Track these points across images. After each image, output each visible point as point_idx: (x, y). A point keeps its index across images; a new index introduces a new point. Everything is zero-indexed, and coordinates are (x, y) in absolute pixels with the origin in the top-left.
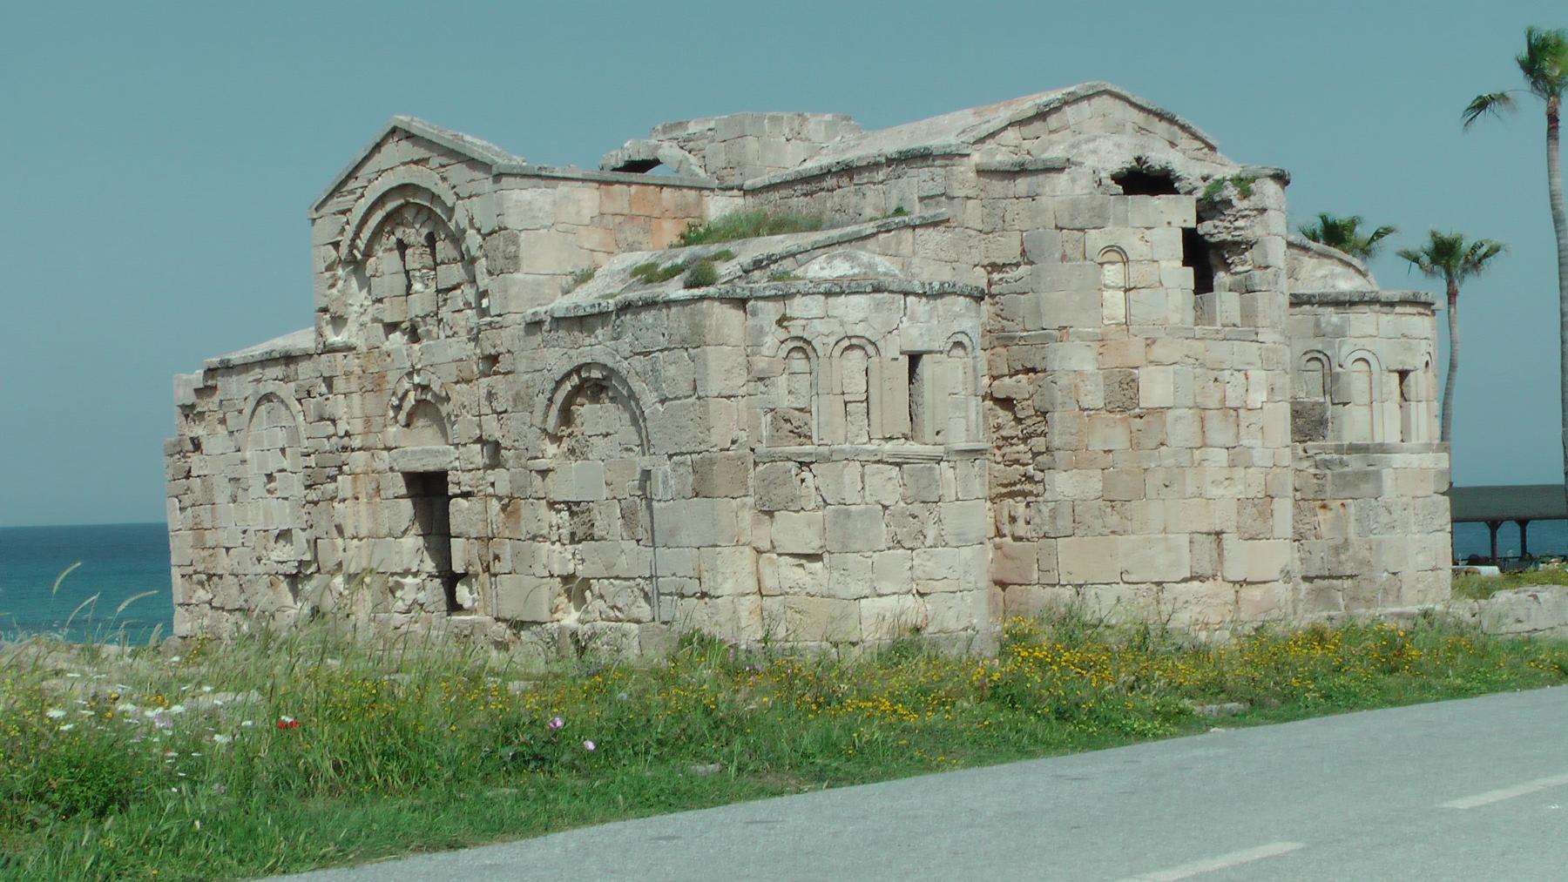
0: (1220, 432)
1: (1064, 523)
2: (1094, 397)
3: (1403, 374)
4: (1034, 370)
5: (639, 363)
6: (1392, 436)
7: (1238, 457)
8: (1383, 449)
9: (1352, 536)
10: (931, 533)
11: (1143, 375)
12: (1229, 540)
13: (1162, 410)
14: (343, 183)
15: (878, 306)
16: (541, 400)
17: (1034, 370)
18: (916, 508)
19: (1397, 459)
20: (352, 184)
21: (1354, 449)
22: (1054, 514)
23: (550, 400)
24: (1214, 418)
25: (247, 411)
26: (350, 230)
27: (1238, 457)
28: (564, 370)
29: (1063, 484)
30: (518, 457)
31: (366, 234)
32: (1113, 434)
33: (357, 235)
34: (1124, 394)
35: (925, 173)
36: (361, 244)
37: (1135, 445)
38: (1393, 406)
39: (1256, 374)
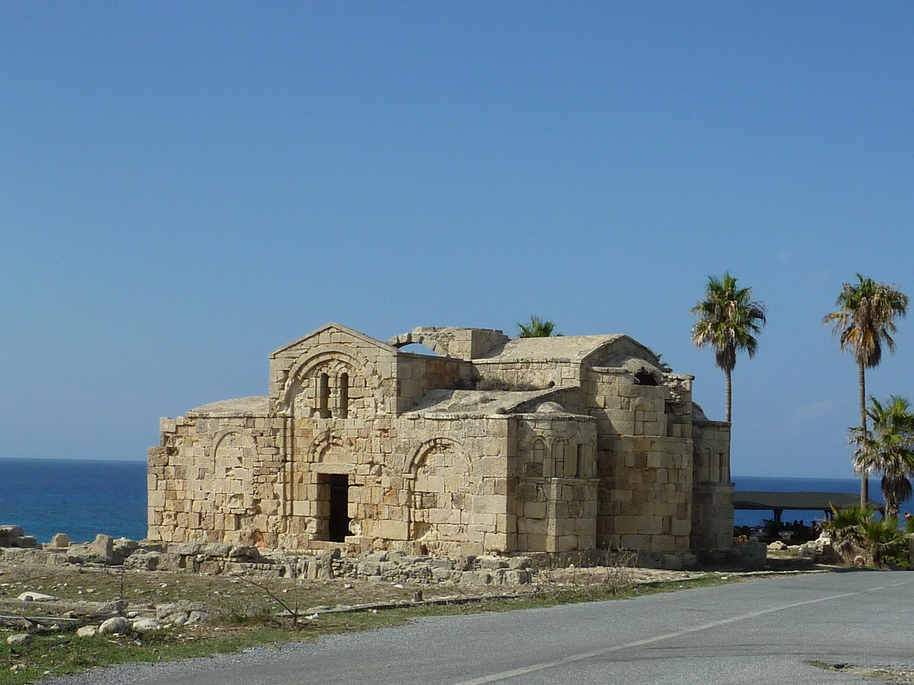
0: (673, 479)
1: (618, 510)
2: (631, 462)
3: (721, 455)
4: (607, 450)
5: (469, 441)
6: (716, 479)
7: (678, 488)
8: (713, 484)
9: (701, 519)
10: (581, 512)
11: (649, 455)
12: (675, 521)
13: (654, 469)
14: (295, 345)
15: (570, 425)
16: (413, 451)
17: (607, 450)
18: (577, 503)
19: (718, 489)
20: (298, 346)
21: (703, 484)
22: (614, 507)
23: (418, 451)
24: (671, 473)
25: (217, 439)
26: (296, 367)
27: (678, 488)
28: (428, 439)
29: (618, 495)
30: (397, 472)
31: (305, 369)
32: (636, 478)
33: (300, 369)
34: (642, 460)
35: (565, 369)
36: (302, 374)
37: (645, 481)
38: (717, 468)
39: (685, 456)
